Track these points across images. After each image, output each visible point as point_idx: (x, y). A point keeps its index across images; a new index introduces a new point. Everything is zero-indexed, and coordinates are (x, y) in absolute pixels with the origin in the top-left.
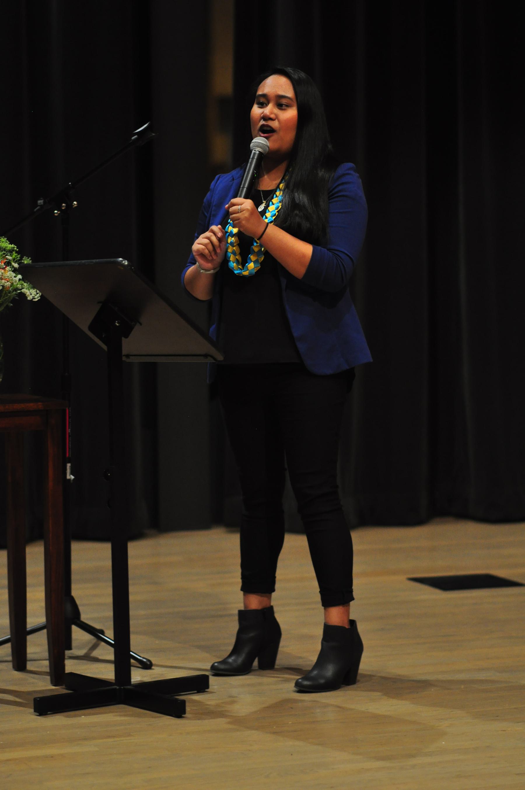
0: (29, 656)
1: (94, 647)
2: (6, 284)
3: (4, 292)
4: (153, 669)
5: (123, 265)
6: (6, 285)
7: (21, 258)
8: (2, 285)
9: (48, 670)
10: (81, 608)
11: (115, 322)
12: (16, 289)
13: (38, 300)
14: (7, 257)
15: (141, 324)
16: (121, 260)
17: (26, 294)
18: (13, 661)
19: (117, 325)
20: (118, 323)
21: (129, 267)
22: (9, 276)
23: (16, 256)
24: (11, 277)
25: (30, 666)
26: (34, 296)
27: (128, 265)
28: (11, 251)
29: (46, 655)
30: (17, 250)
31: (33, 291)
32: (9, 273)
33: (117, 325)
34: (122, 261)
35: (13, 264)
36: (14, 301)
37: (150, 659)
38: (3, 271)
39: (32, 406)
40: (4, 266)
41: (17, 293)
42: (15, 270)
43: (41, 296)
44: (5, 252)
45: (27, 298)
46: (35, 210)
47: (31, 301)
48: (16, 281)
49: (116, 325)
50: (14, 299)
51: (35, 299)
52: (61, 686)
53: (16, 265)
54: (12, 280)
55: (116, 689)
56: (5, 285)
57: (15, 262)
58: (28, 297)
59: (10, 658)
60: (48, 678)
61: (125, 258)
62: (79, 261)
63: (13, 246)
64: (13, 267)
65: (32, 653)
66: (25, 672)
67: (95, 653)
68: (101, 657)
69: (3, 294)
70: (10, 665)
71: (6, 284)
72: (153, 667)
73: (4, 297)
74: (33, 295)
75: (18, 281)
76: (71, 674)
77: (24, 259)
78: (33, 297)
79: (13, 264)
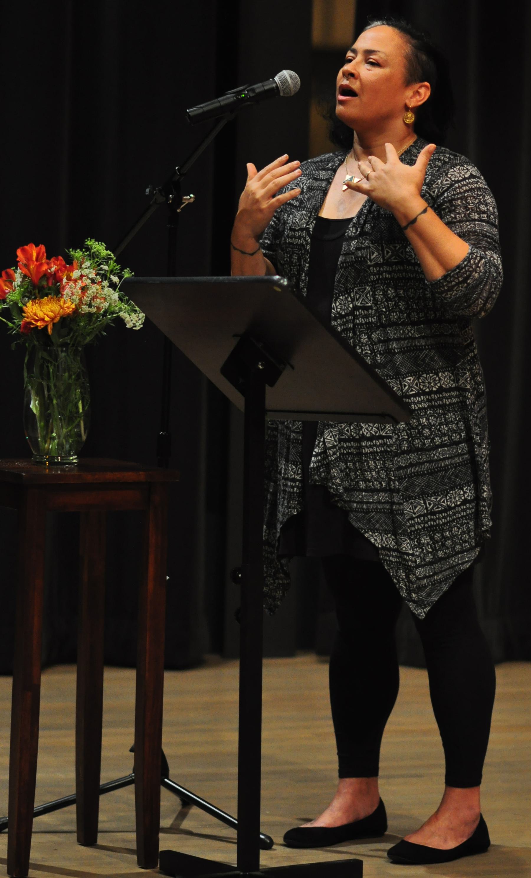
0: (100, 826)
1: (182, 816)
2: (102, 305)
3: (95, 316)
4: (275, 850)
5: (281, 286)
6: (103, 307)
7: (122, 269)
8: (96, 306)
9: (134, 846)
10: (169, 761)
11: (258, 364)
12: (112, 313)
13: (141, 328)
14: (102, 266)
15: (293, 368)
16: (279, 279)
17: (125, 320)
18: (79, 831)
19: (261, 367)
20: (262, 365)
21: (290, 289)
22: (107, 294)
23: (115, 266)
24: (109, 296)
25: (101, 840)
26: (135, 322)
27: (288, 286)
28: (107, 259)
29: (132, 824)
30: (115, 258)
31: (134, 316)
32: (108, 291)
33: (261, 367)
34: (279, 280)
35: (112, 277)
36: (107, 328)
37: (270, 836)
38: (98, 287)
39: (130, 476)
40: (100, 280)
41: (113, 318)
42: (113, 286)
43: (147, 323)
44: (98, 260)
45: (126, 325)
46: (151, 203)
47: (131, 329)
48: (115, 302)
49: (259, 368)
50: (108, 326)
51: (135, 326)
52: (152, 869)
53: (115, 279)
54: (111, 299)
55: (238, 875)
56: (101, 307)
57: (114, 275)
58: (127, 324)
59: (74, 827)
60: (135, 857)
61: (283, 276)
62: (215, 278)
63: (109, 252)
64: (110, 281)
65: (104, 821)
66: (94, 848)
67: (186, 824)
68: (195, 831)
69: (94, 319)
70: (75, 836)
71: (102, 305)
72: (274, 847)
73: (94, 323)
74: (134, 322)
75: (118, 302)
76: (169, 853)
77: (125, 270)
78: (134, 324)
79: (112, 277)
